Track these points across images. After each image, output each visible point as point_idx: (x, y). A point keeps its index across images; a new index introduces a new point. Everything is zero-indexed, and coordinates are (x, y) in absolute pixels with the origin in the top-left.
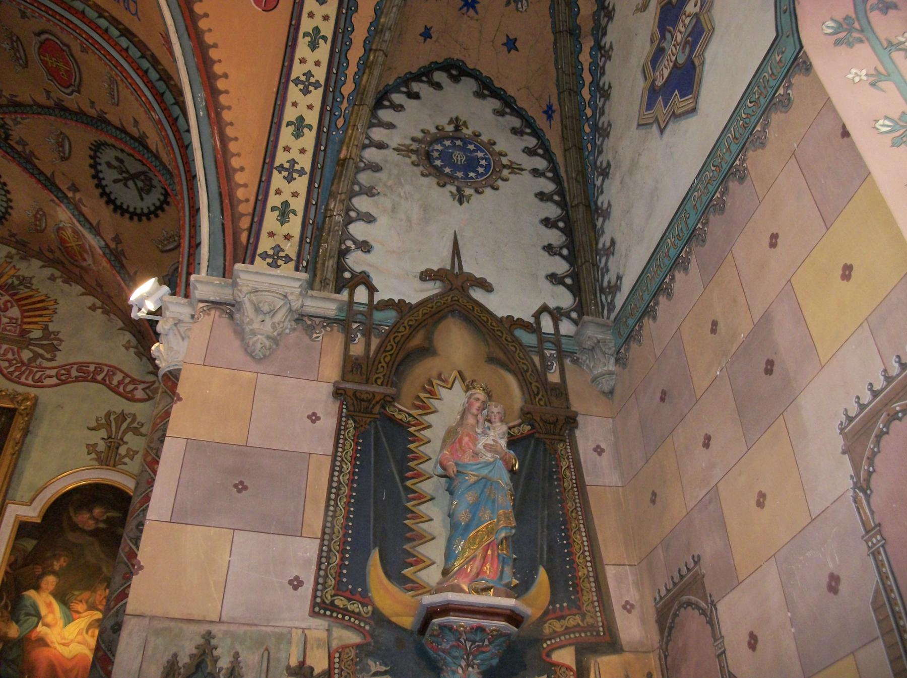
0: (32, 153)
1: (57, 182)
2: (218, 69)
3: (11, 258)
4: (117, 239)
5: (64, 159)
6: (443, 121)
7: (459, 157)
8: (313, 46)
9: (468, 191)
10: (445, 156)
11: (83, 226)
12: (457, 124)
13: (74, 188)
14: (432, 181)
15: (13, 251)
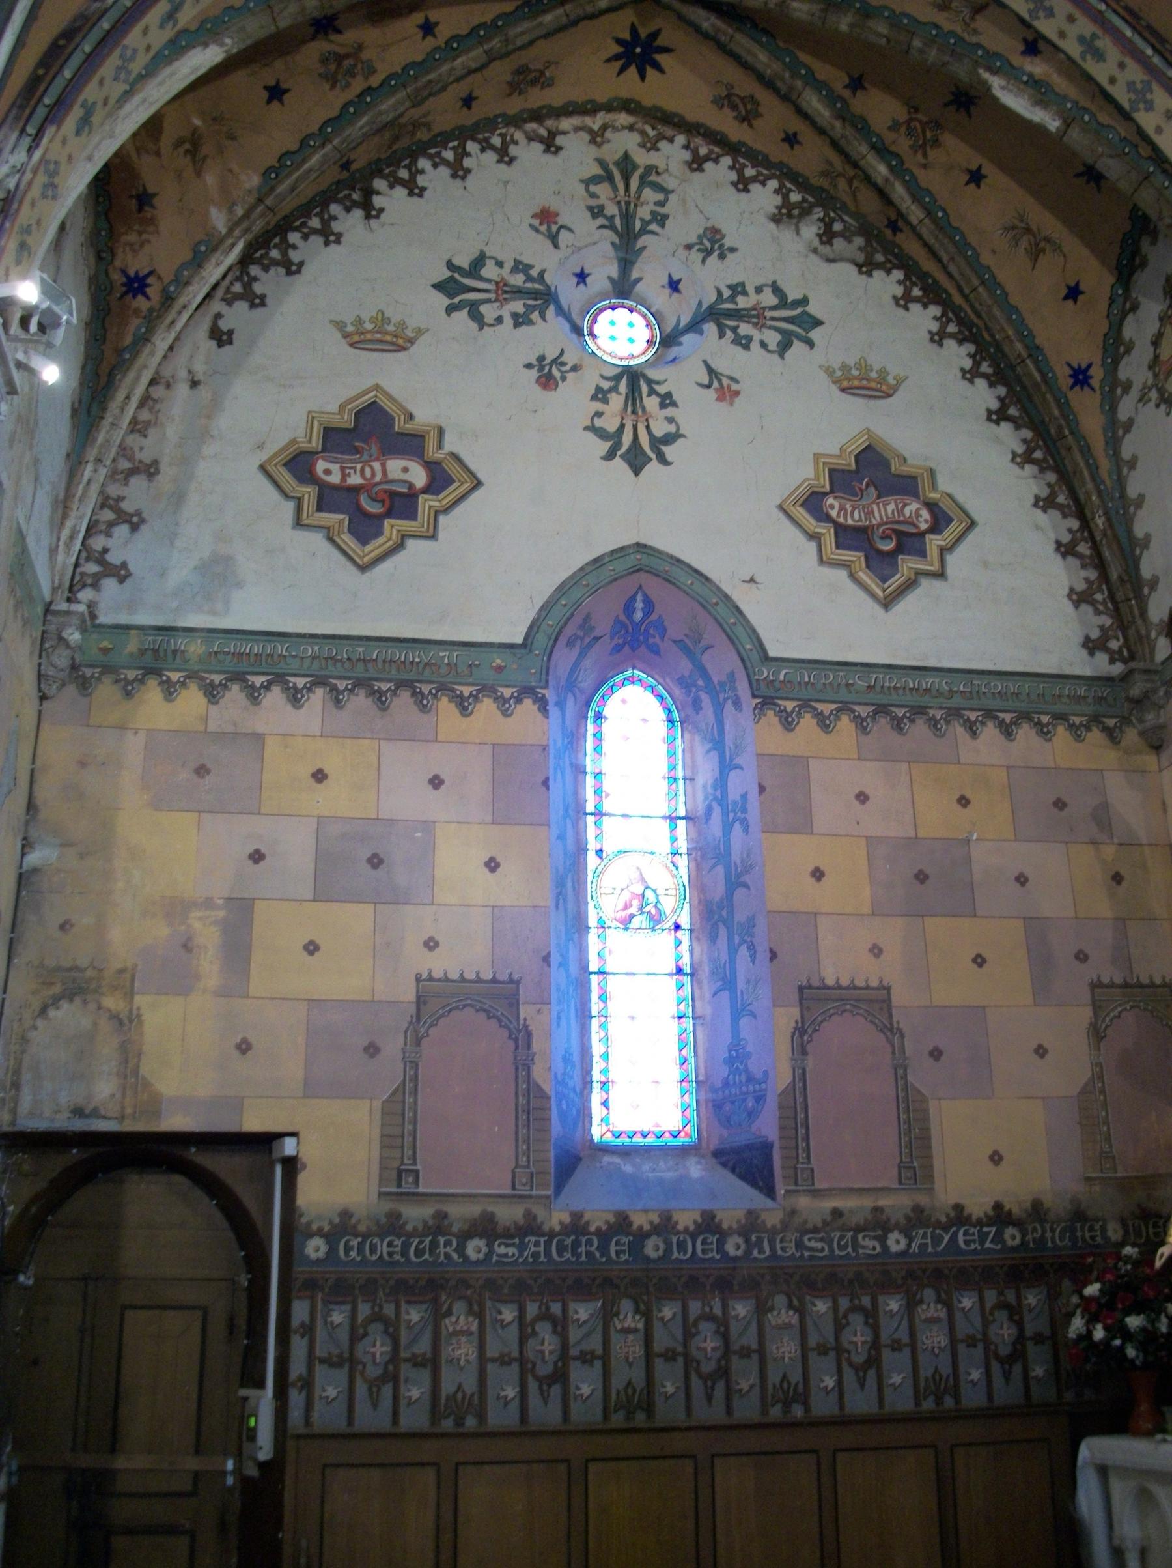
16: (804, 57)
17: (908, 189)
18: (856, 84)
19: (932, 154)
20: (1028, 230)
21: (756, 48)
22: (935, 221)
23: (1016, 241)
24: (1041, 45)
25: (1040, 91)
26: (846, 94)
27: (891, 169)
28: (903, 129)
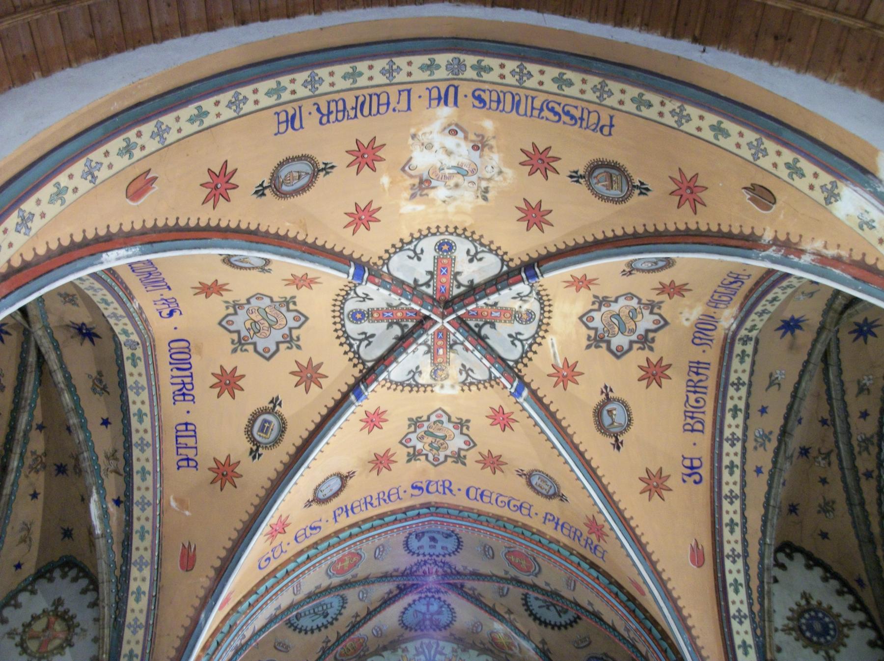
0: (480, 594)
1: (497, 609)
2: (685, 612)
3: (456, 652)
4: (543, 642)
5: (502, 596)
6: (798, 598)
7: (817, 626)
8: (737, 591)
9: (832, 652)
10: (810, 628)
11: (519, 636)
12: (806, 596)
13: (510, 612)
14: (809, 651)
15: (455, 646)
16: (39, 401)
17: (14, 479)
18: (41, 427)
19: (33, 474)
20: (29, 530)
21: (32, 382)
22: (10, 498)
23: (22, 529)
24: (122, 505)
25: (105, 515)
26: (34, 426)
27: (18, 467)
28: (34, 457)
